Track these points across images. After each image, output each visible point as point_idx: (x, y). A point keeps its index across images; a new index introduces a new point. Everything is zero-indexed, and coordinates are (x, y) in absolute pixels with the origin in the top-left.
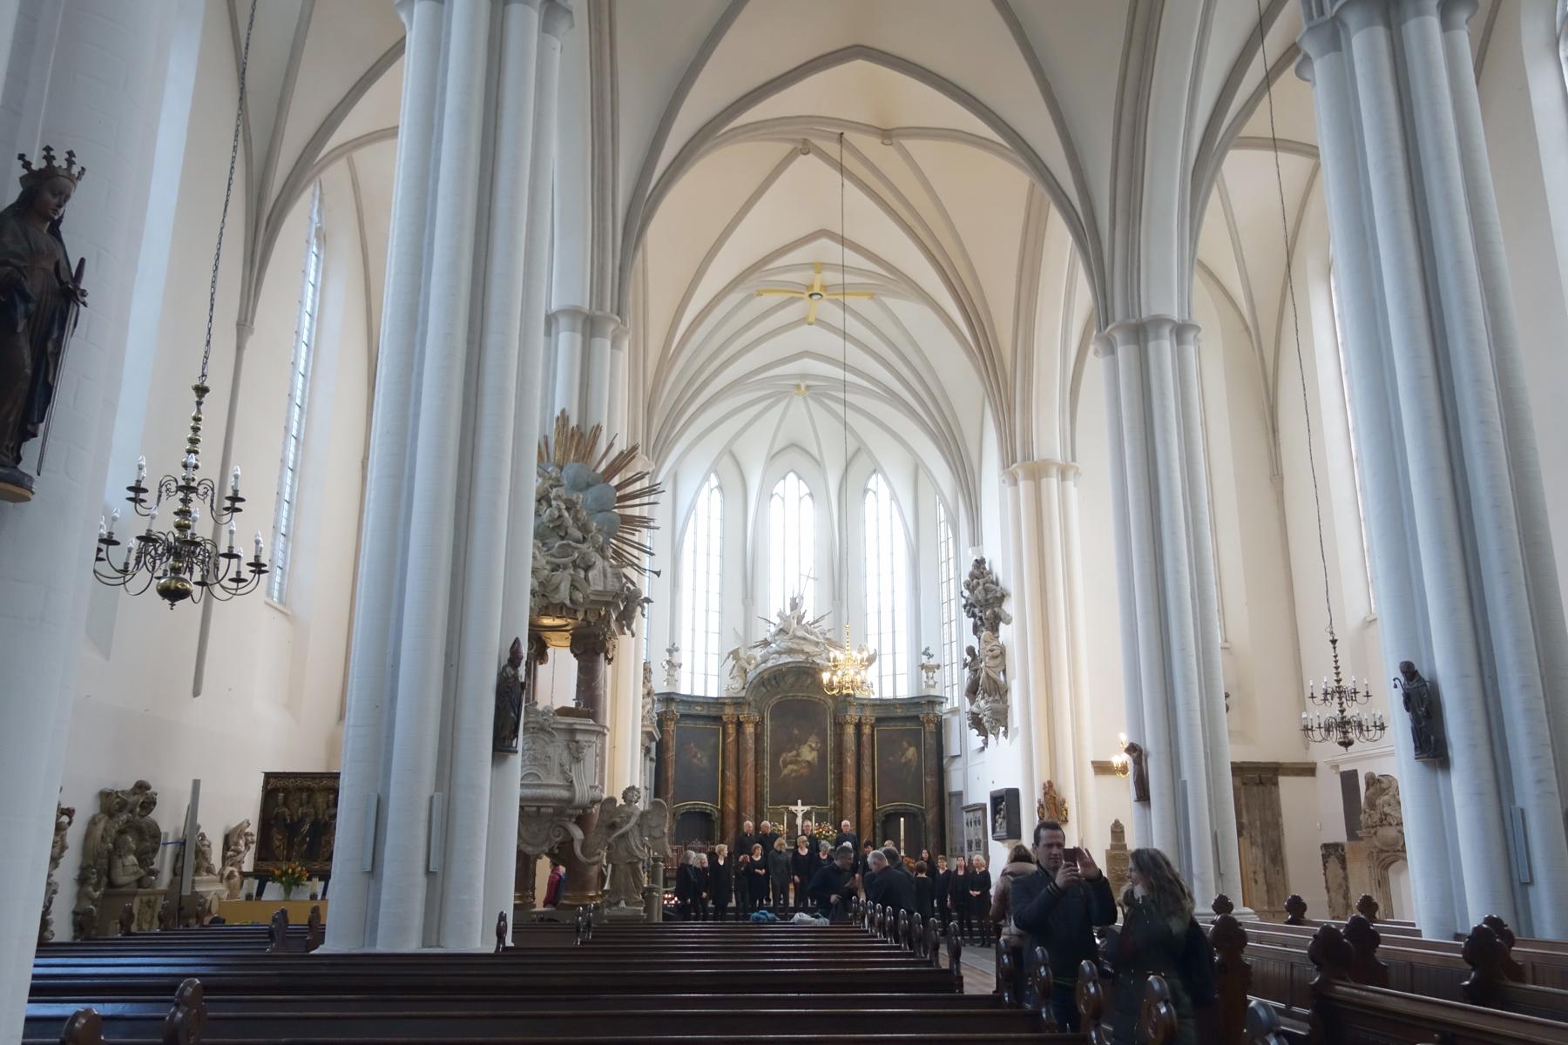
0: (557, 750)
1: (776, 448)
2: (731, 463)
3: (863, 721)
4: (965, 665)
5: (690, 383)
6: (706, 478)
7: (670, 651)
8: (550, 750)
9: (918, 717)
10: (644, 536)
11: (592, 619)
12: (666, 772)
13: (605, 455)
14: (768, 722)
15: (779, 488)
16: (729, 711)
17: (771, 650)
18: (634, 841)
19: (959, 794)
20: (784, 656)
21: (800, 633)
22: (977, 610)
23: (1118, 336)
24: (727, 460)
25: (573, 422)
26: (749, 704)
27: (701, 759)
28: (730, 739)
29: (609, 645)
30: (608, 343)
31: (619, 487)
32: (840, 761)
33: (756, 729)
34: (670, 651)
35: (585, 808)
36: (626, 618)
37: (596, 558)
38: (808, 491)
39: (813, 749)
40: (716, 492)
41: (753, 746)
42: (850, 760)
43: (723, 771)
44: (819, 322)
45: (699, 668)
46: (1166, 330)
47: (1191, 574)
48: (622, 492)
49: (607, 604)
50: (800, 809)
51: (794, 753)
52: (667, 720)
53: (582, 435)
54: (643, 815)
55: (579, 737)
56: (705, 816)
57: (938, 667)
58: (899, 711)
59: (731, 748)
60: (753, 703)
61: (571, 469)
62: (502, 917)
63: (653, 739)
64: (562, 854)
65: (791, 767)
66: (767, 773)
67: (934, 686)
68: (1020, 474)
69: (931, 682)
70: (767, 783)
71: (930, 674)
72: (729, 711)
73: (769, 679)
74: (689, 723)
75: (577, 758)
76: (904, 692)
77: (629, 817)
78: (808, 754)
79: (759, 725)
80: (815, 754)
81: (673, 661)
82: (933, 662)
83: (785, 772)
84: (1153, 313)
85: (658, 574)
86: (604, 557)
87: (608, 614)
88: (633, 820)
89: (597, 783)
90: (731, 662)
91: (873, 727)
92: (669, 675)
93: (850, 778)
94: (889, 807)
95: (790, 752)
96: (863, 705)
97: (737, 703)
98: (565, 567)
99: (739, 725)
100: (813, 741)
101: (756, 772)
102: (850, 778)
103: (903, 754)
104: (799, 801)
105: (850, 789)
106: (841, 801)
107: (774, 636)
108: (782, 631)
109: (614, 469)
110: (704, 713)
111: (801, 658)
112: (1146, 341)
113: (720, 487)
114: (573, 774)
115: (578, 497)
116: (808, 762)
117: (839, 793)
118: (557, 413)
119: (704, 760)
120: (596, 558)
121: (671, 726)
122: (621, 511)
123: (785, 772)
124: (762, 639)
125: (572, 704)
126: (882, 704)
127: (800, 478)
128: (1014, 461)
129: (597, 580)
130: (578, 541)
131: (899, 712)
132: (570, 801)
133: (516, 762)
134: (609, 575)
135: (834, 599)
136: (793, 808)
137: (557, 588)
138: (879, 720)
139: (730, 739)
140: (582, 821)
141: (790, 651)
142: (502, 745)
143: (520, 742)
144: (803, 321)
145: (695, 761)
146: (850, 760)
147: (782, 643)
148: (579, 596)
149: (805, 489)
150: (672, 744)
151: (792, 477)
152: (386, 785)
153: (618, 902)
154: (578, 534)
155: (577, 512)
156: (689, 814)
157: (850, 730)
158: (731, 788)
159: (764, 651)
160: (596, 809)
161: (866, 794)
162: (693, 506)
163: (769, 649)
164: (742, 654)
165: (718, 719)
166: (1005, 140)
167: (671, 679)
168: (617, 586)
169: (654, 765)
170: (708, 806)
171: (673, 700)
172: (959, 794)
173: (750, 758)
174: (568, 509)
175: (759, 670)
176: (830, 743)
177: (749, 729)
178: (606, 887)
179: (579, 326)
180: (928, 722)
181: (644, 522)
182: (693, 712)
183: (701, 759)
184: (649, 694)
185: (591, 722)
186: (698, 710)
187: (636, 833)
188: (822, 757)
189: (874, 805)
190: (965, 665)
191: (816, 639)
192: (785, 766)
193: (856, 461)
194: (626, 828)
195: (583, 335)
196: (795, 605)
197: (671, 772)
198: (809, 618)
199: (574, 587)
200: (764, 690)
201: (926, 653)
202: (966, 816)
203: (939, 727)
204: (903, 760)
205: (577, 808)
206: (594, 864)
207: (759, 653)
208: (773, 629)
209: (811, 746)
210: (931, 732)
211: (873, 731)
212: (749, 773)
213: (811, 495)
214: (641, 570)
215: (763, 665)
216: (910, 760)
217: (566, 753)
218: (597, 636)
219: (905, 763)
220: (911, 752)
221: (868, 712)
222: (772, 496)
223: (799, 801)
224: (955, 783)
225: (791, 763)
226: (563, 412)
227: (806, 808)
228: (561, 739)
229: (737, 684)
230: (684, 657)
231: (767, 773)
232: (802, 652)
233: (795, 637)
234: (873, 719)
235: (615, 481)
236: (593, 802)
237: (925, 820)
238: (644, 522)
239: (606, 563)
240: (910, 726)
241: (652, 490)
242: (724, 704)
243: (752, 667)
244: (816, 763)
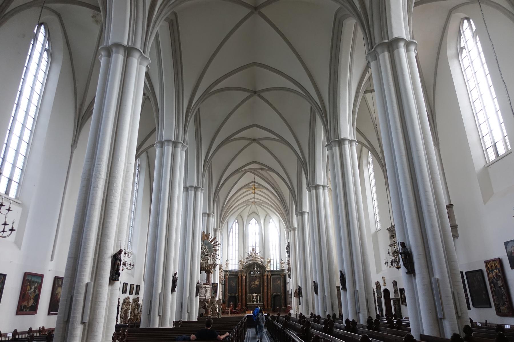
1: (250, 213)
3: (268, 275)
4: (287, 264)
6: (235, 221)
7: (227, 261)
8: (202, 291)
9: (280, 274)
11: (209, 268)
12: (226, 287)
13: (211, 238)
14: (248, 276)
15: (251, 222)
16: (240, 273)
17: (248, 260)
18: (216, 305)
19: (289, 291)
20: (251, 261)
21: (255, 256)
22: (289, 253)
23: (298, 214)
24: (239, 217)
25: (205, 233)
26: (244, 272)
27: (234, 284)
28: (240, 280)
29: (211, 271)
30: (211, 218)
31: (213, 244)
33: (245, 277)
34: (227, 261)
35: (208, 300)
36: (214, 267)
37: (210, 258)
38: (257, 222)
39: (258, 282)
40: (237, 224)
41: (245, 281)
42: (266, 284)
43: (238, 287)
44: (255, 193)
45: (234, 263)
46: (306, 214)
47: (310, 256)
48: (213, 245)
49: (211, 266)
50: (255, 295)
51: (254, 282)
52: (226, 276)
53: (207, 235)
54: (217, 301)
55: (207, 288)
56: (234, 297)
57: (284, 263)
58: (276, 273)
59: (240, 282)
60: (245, 272)
62: (197, 317)
63: (223, 281)
64: (205, 307)
65: (253, 286)
66: (248, 287)
67: (283, 267)
68: (291, 230)
69: (283, 266)
70: (248, 289)
71: (283, 265)
72: (240, 273)
73: (248, 266)
74: (231, 276)
75: (206, 291)
76: (278, 269)
77: (215, 301)
78: (257, 283)
79: (246, 277)
80: (258, 282)
81: (227, 263)
82: (283, 262)
83: (252, 287)
84: (304, 211)
85: (220, 259)
86: (211, 257)
87: (211, 267)
88: (216, 302)
89: (210, 296)
90: (240, 263)
91: (271, 276)
92: (226, 266)
93: (266, 288)
94: (274, 294)
95: (253, 282)
96: (268, 272)
97: (241, 272)
98: (204, 260)
99: (242, 277)
100: (258, 280)
101: (245, 287)
102: (266, 288)
103: (277, 282)
104: (255, 293)
105: (265, 290)
106: (264, 293)
107: (249, 257)
108: (251, 255)
110: (234, 274)
111: (255, 262)
112: (303, 215)
113: (238, 222)
114: (206, 294)
116: (257, 284)
117: (263, 291)
118: (203, 231)
119: (234, 284)
120: (210, 258)
121: (227, 277)
122: (213, 248)
123: (252, 287)
124: (247, 257)
125: (206, 283)
126: (273, 271)
127: (255, 219)
128: (290, 227)
129: (210, 262)
130: (206, 255)
131: (276, 273)
132: (206, 299)
133: (198, 297)
134: (211, 260)
135: (263, 247)
136: (253, 295)
137: (203, 264)
138: (272, 275)
139: (240, 280)
140: (207, 302)
141: (252, 260)
142: (197, 295)
143: (199, 294)
144: (252, 193)
145: (232, 285)
146: (266, 284)
147: (251, 258)
148: (207, 265)
149: (256, 222)
150: (227, 281)
151: (254, 219)
152: (183, 301)
153: (213, 316)
154: (206, 254)
155: (206, 250)
157: (266, 277)
158: (240, 290)
159: (247, 260)
160: (209, 300)
161: (269, 291)
162: (232, 227)
163: (248, 260)
164: (243, 261)
165: (237, 275)
166: (321, 105)
167: (227, 267)
168: (213, 262)
169: (223, 286)
170: (235, 295)
171: (227, 272)
172: (289, 291)
173: (244, 284)
174: (205, 249)
175: (246, 265)
177: (244, 277)
178: (212, 313)
179: (206, 216)
180: (282, 275)
181: (217, 250)
182: (232, 274)
183: (234, 284)
184: (222, 272)
185: (209, 285)
186: (233, 273)
187: (216, 304)
188: (260, 283)
189: (271, 294)
190: (287, 264)
191: (258, 257)
192: (252, 285)
193: (267, 216)
194: (214, 303)
195: (207, 217)
196: (253, 250)
197: (227, 287)
198: (257, 252)
200: (247, 269)
201: (282, 260)
202: (290, 296)
203: (285, 276)
204: (277, 284)
205: (207, 300)
206: (209, 309)
207: (245, 260)
208: (249, 255)
209: (257, 281)
210: (283, 277)
211: (271, 277)
212: (244, 288)
213: (258, 223)
214: (216, 258)
215: (247, 263)
216: (278, 284)
217: (205, 291)
218: (210, 270)
219: (278, 285)
220: (279, 282)
221: (269, 273)
222: (249, 223)
223: (255, 293)
224: (288, 289)
225: (253, 285)
226: (204, 231)
227: (256, 295)
228: (204, 289)
229: (241, 267)
230: (230, 262)
231: (248, 287)
232: (255, 260)
233: (253, 257)
234: (271, 275)
235: (212, 243)
236: (209, 299)
237: (282, 297)
238: (217, 250)
239: (211, 258)
240: (279, 276)
241: (218, 244)
242: (238, 272)
243: (244, 264)
244: (259, 284)
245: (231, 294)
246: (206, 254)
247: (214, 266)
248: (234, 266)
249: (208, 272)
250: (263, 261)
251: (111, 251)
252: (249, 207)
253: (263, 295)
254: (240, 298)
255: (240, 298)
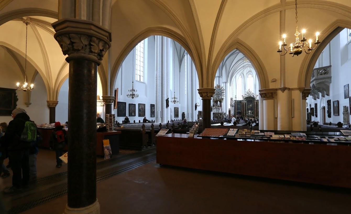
0: (218, 109)
2: (243, 75)
5: (235, 69)
10: (224, 93)
18: (223, 115)
30: (221, 78)
32: (254, 106)
36: (222, 100)
37: (220, 96)
42: (255, 106)
50: (250, 111)
56: (240, 112)
61: (218, 89)
70: (246, 108)
75: (219, 110)
78: (251, 106)
79: (245, 104)
97: (242, 101)
105: (255, 109)
108: (248, 93)
109: (221, 88)
111: (250, 96)
115: (219, 91)
117: (254, 109)
120: (220, 96)
141: (248, 95)
144: (246, 62)
146: (255, 106)
147: (248, 94)
151: (250, 75)
154: (219, 94)
156: (238, 112)
157: (255, 103)
164: (243, 96)
165: (241, 103)
170: (240, 111)
173: (244, 106)
176: (253, 104)
181: (223, 92)
183: (239, 106)
186: (239, 102)
197: (236, 108)
199: (218, 98)
230: (237, 96)
238: (223, 92)
245: (238, 111)
246: (219, 94)
247: (223, 99)
248: (240, 98)
249: (221, 102)
250: (254, 95)
251: (165, 98)
252: (246, 69)
253: (254, 111)
254: (242, 113)
255: (242, 113)
